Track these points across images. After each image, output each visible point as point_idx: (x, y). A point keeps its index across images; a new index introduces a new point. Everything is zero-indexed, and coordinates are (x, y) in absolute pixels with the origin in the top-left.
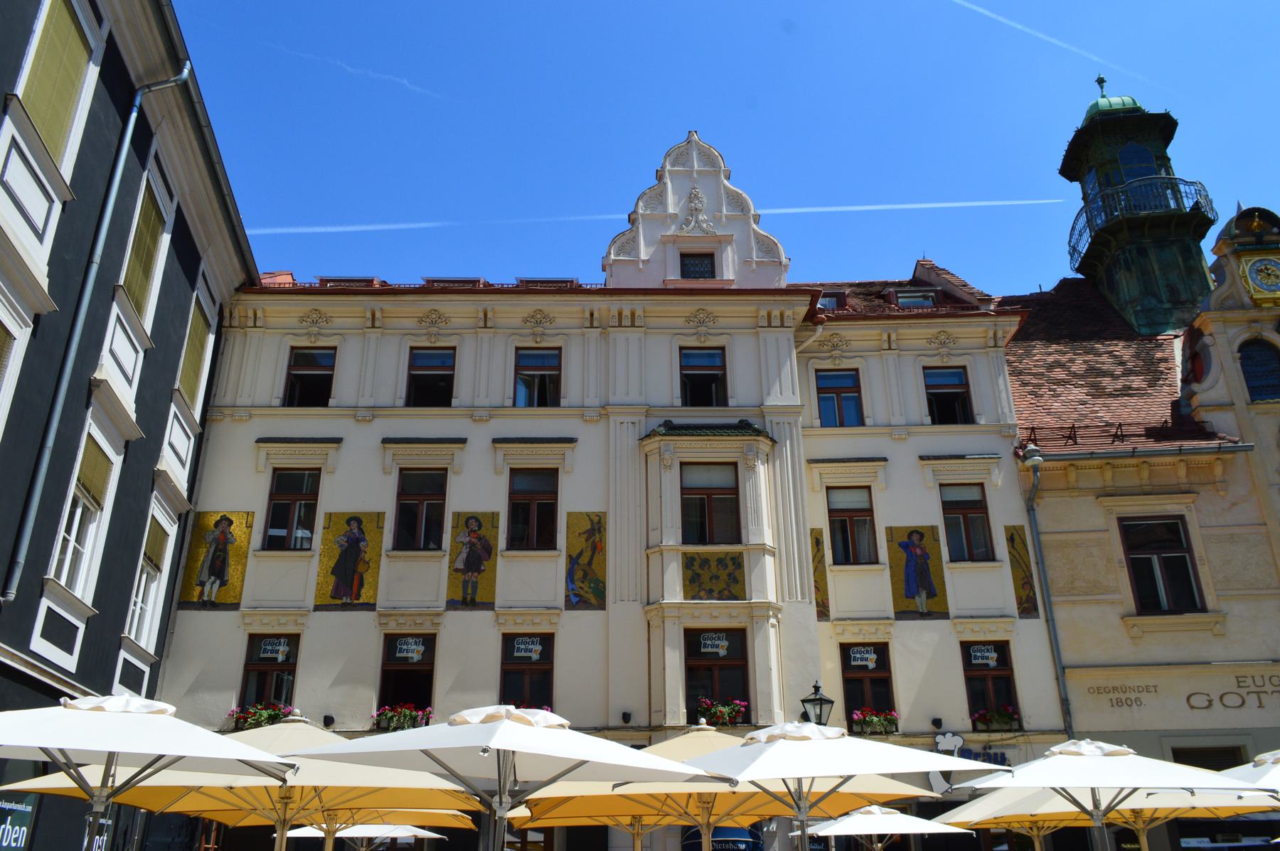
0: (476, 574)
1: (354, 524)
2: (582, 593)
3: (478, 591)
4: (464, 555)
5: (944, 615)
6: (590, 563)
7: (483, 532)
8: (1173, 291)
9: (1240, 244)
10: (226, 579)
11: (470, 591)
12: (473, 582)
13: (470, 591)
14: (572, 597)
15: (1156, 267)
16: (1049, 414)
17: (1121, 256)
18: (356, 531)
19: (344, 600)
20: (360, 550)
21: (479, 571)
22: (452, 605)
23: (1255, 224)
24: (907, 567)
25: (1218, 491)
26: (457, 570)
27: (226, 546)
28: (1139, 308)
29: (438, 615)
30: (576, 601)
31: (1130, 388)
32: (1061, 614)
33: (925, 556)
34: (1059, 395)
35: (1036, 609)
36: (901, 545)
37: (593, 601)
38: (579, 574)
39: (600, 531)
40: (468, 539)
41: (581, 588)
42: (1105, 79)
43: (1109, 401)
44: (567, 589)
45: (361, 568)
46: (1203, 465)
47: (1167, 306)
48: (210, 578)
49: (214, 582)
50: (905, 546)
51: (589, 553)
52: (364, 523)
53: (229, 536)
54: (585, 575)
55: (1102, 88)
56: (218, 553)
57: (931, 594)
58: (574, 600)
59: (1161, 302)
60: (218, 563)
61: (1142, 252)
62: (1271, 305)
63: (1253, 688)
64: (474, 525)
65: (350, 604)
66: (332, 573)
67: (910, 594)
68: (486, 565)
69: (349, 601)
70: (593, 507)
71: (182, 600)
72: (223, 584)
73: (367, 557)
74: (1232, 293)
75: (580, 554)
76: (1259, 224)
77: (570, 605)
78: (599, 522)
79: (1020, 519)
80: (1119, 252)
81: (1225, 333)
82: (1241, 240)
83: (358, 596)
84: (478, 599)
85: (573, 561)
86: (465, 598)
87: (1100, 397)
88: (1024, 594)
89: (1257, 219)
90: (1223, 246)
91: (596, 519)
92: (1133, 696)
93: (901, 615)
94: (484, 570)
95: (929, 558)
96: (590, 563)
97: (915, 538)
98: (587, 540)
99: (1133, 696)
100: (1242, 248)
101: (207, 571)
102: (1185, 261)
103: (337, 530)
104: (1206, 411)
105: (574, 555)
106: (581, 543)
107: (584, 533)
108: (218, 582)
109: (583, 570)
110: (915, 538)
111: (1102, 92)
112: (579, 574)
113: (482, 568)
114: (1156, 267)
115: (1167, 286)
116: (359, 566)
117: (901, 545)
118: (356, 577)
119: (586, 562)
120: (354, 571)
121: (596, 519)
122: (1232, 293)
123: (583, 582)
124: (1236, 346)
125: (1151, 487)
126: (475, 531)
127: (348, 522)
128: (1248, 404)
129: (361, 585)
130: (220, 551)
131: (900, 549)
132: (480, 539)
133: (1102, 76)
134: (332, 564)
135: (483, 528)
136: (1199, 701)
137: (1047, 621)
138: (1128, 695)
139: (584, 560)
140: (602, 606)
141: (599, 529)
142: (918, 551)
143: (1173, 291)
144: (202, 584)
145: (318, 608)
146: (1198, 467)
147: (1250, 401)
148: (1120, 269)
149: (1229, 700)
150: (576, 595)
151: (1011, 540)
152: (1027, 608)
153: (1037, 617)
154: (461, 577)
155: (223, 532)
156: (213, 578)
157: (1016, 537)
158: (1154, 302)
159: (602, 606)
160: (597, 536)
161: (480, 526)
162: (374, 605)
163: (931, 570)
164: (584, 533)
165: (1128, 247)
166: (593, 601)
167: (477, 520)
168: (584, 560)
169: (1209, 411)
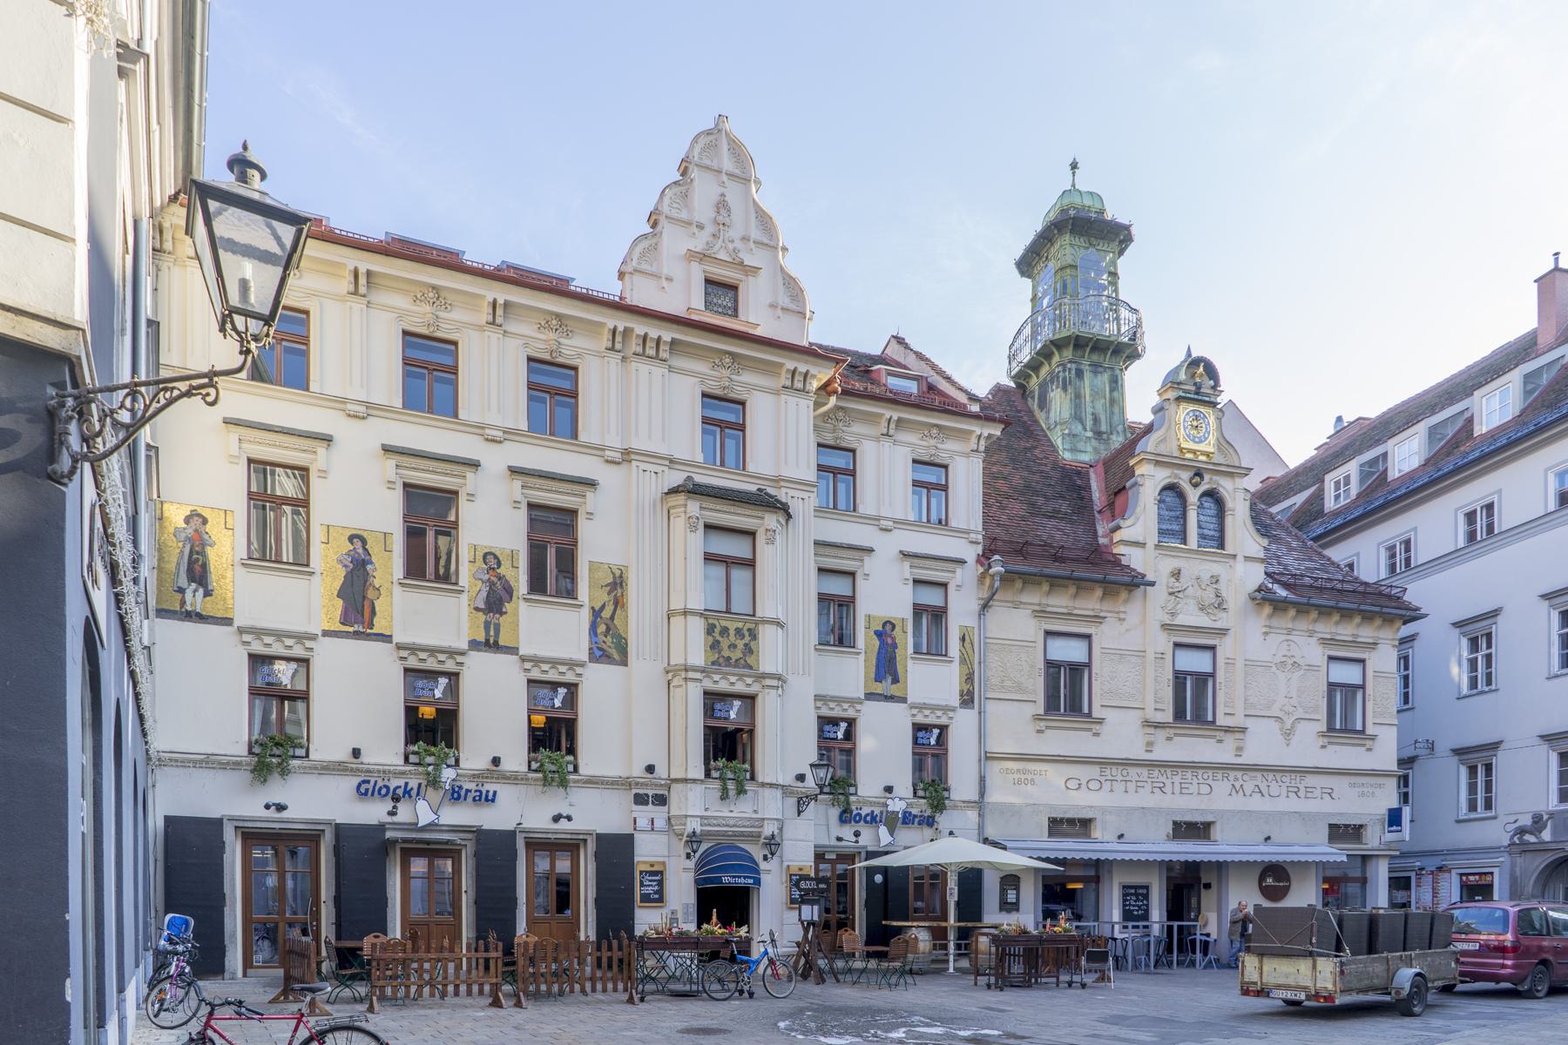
0: (498, 616)
1: (358, 544)
2: (605, 647)
3: (501, 633)
4: (484, 594)
5: (903, 700)
6: (612, 618)
7: (502, 571)
8: (1096, 420)
10: (210, 588)
11: (492, 633)
12: (495, 624)
13: (492, 633)
14: (595, 649)
15: (1088, 392)
16: (998, 525)
17: (1061, 374)
18: (360, 551)
19: (356, 628)
20: (368, 574)
21: (502, 614)
22: (474, 645)
24: (879, 653)
26: (477, 609)
27: (203, 548)
28: (1067, 432)
29: (462, 654)
30: (599, 655)
31: (1059, 512)
32: (992, 707)
33: (895, 646)
34: (1004, 508)
35: (973, 702)
36: (876, 633)
37: (616, 656)
38: (602, 628)
39: (621, 586)
40: (487, 577)
41: (604, 642)
43: (1045, 521)
44: (591, 641)
45: (370, 594)
47: (1089, 434)
48: (190, 585)
49: (195, 591)
50: (879, 634)
51: (612, 608)
52: (369, 542)
53: (206, 537)
54: (608, 629)
56: (195, 556)
57: (896, 680)
58: (598, 653)
59: (1085, 430)
60: (197, 568)
61: (1080, 374)
63: (1110, 778)
64: (493, 563)
65: (363, 633)
66: (338, 596)
67: (878, 679)
68: (508, 607)
69: (361, 629)
70: (615, 559)
71: (160, 607)
72: (208, 593)
73: (377, 583)
75: (603, 607)
77: (593, 658)
78: (621, 577)
79: (972, 622)
80: (1060, 368)
83: (371, 626)
84: (501, 643)
85: (596, 614)
86: (487, 641)
87: (1037, 515)
88: (966, 688)
91: (618, 573)
92: (1029, 777)
93: (870, 696)
94: (506, 613)
95: (896, 648)
96: (612, 618)
97: (888, 627)
98: (609, 594)
99: (1029, 777)
101: (185, 576)
102: (1112, 391)
103: (338, 546)
105: (597, 609)
106: (603, 597)
107: (606, 586)
108: (201, 591)
109: (606, 624)
110: (888, 627)
112: (602, 628)
113: (504, 610)
114: (1088, 392)
115: (1093, 414)
116: (369, 592)
117: (876, 633)
118: (366, 603)
119: (608, 616)
120: (364, 597)
121: (618, 573)
123: (606, 636)
126: (493, 569)
127: (351, 539)
129: (373, 613)
130: (198, 553)
131: (875, 637)
132: (500, 578)
134: (338, 584)
135: (502, 567)
136: (1072, 784)
137: (980, 713)
138: (1026, 776)
139: (606, 614)
140: (624, 662)
141: (621, 583)
142: (889, 641)
143: (1096, 420)
144: (181, 591)
145: (326, 633)
148: (1057, 388)
149: (1091, 785)
150: (600, 649)
151: (963, 639)
152: (967, 700)
153: (973, 708)
154: (482, 617)
155: (196, 531)
156: (194, 585)
157: (967, 637)
158: (1080, 427)
159: (624, 662)
160: (619, 590)
161: (499, 564)
162: (391, 636)
163: (898, 659)
164: (606, 586)
165: (1069, 365)
166: (616, 656)
167: (496, 557)
168: (606, 614)
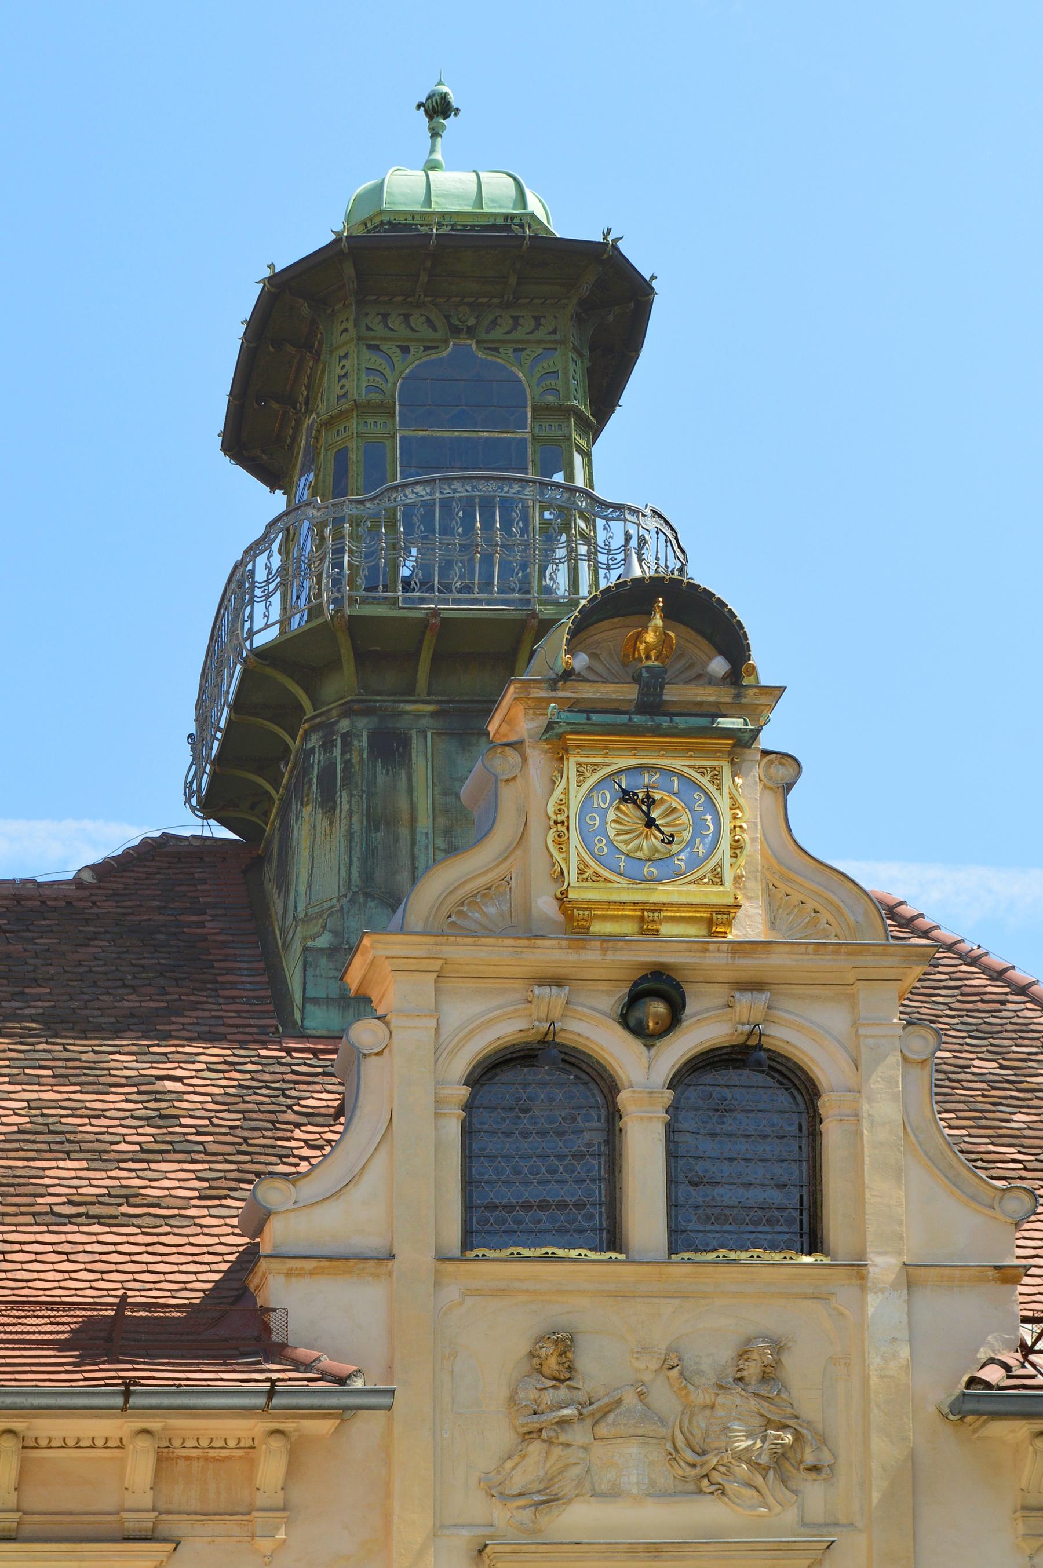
9: (574, 706)
23: (650, 637)
25: (253, 1537)
42: (454, 102)
46: (224, 1453)
55: (435, 134)
62: (628, 928)
74: (506, 880)
76: (664, 639)
81: (436, 1012)
82: (587, 692)
89: (658, 621)
90: (519, 710)
100: (581, 718)
104: (289, 1274)
111: (432, 151)
122: (506, 880)
124: (461, 1065)
125: (16, 1516)
128: (443, 1258)
133: (444, 89)
146: (206, 1459)
147: (456, 1251)
169: (300, 1273)
